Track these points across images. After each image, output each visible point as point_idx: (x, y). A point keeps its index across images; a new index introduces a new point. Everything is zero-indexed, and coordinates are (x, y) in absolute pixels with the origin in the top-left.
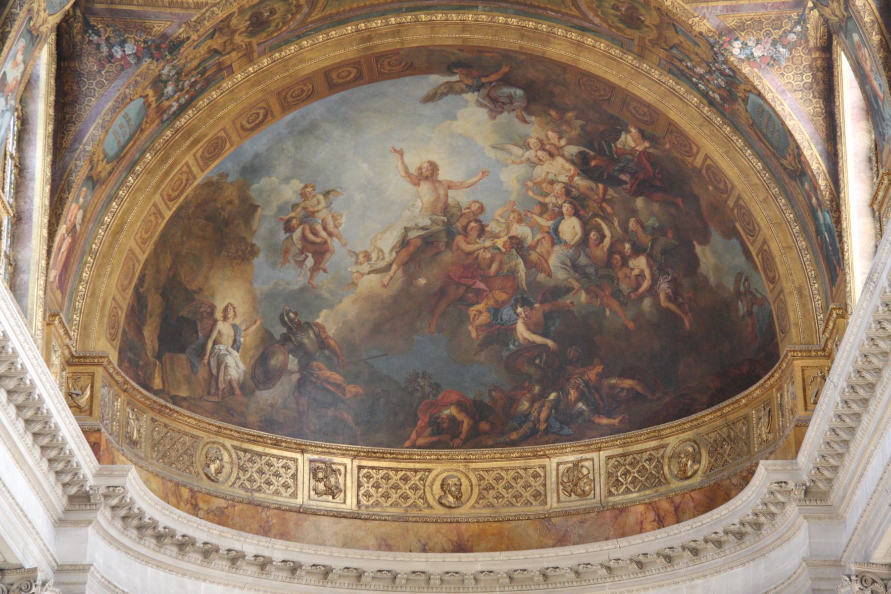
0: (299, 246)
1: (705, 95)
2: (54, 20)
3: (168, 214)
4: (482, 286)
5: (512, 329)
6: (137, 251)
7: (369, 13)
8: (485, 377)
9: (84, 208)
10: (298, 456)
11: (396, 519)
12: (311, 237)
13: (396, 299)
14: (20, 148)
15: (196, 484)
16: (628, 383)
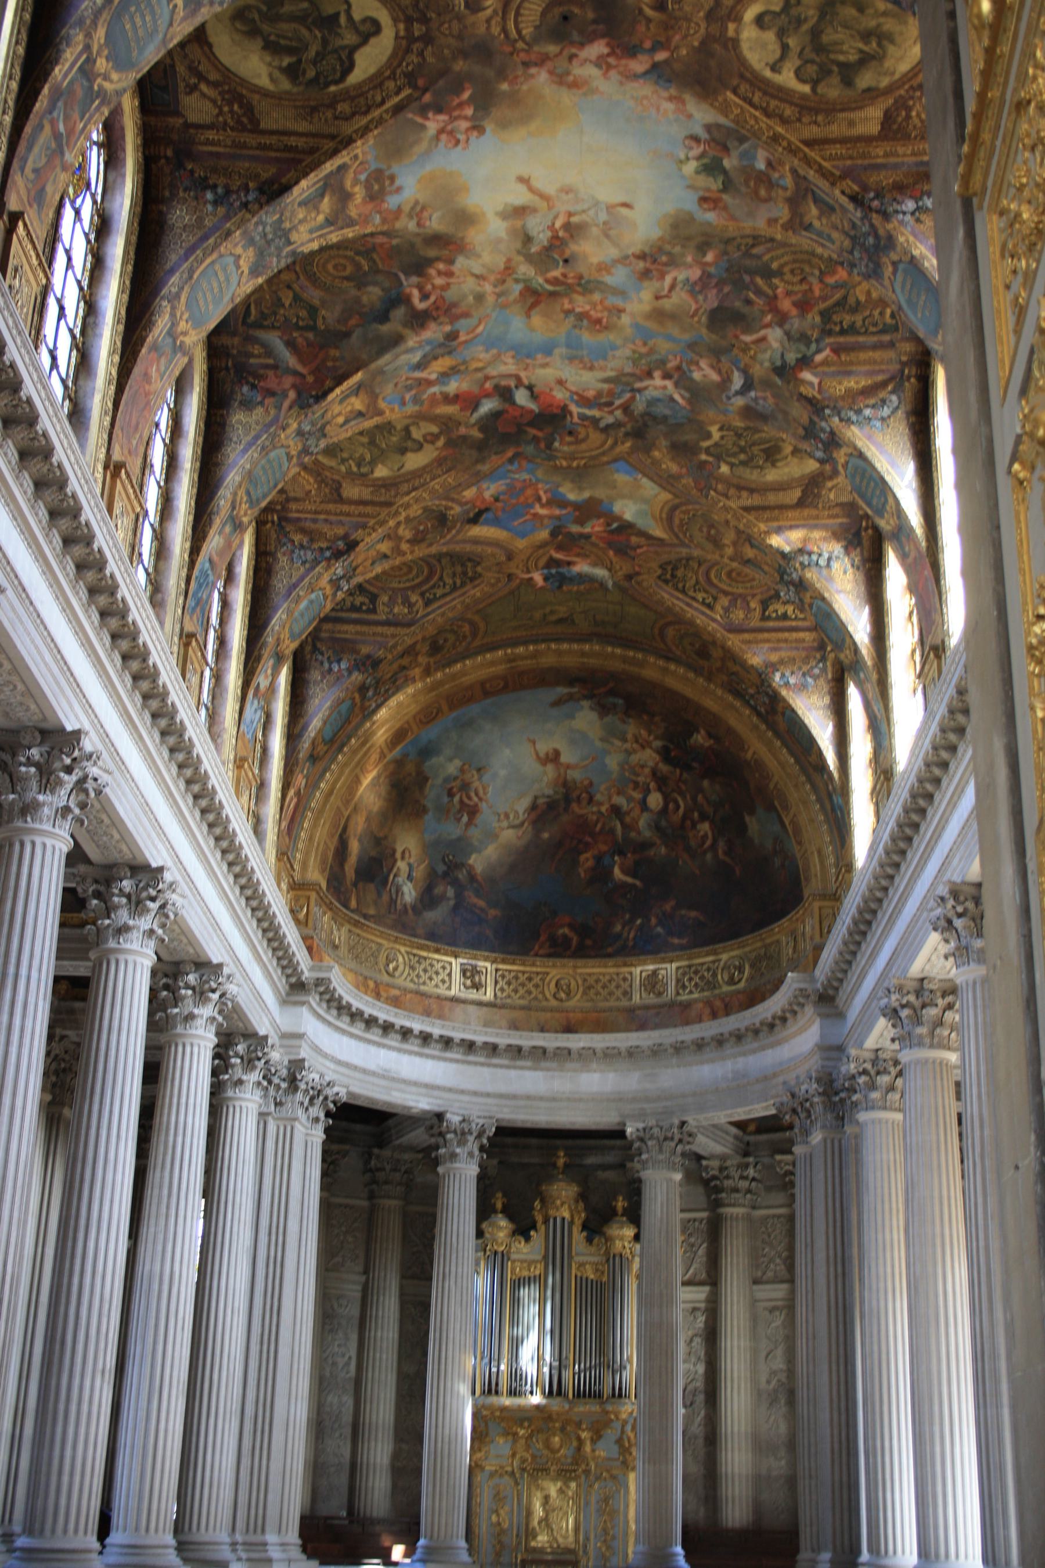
0: (458, 806)
1: (754, 709)
2: (294, 645)
4: (588, 839)
5: (612, 872)
6: (343, 809)
7: (515, 643)
9: (307, 777)
10: (453, 960)
11: (522, 1008)
12: (466, 800)
14: (264, 735)
15: (378, 977)
16: (693, 914)
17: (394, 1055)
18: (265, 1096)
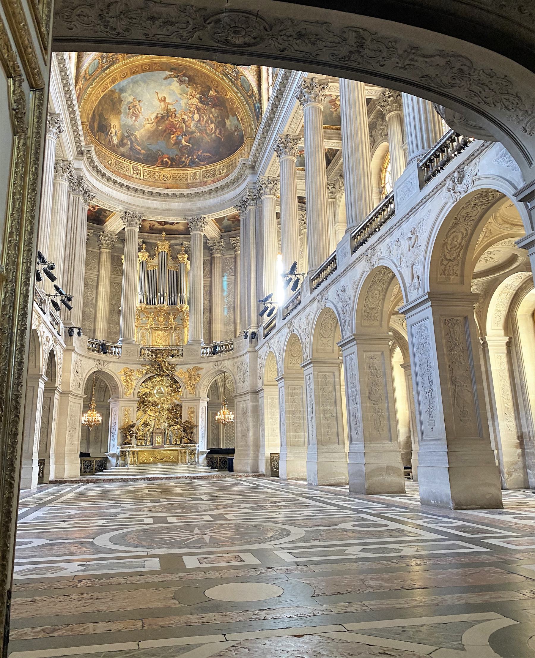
1: (230, 80)
3: (102, 95)
8: (175, 153)
13: (154, 131)
16: (208, 154)
17: (111, 190)
18: (70, 186)
